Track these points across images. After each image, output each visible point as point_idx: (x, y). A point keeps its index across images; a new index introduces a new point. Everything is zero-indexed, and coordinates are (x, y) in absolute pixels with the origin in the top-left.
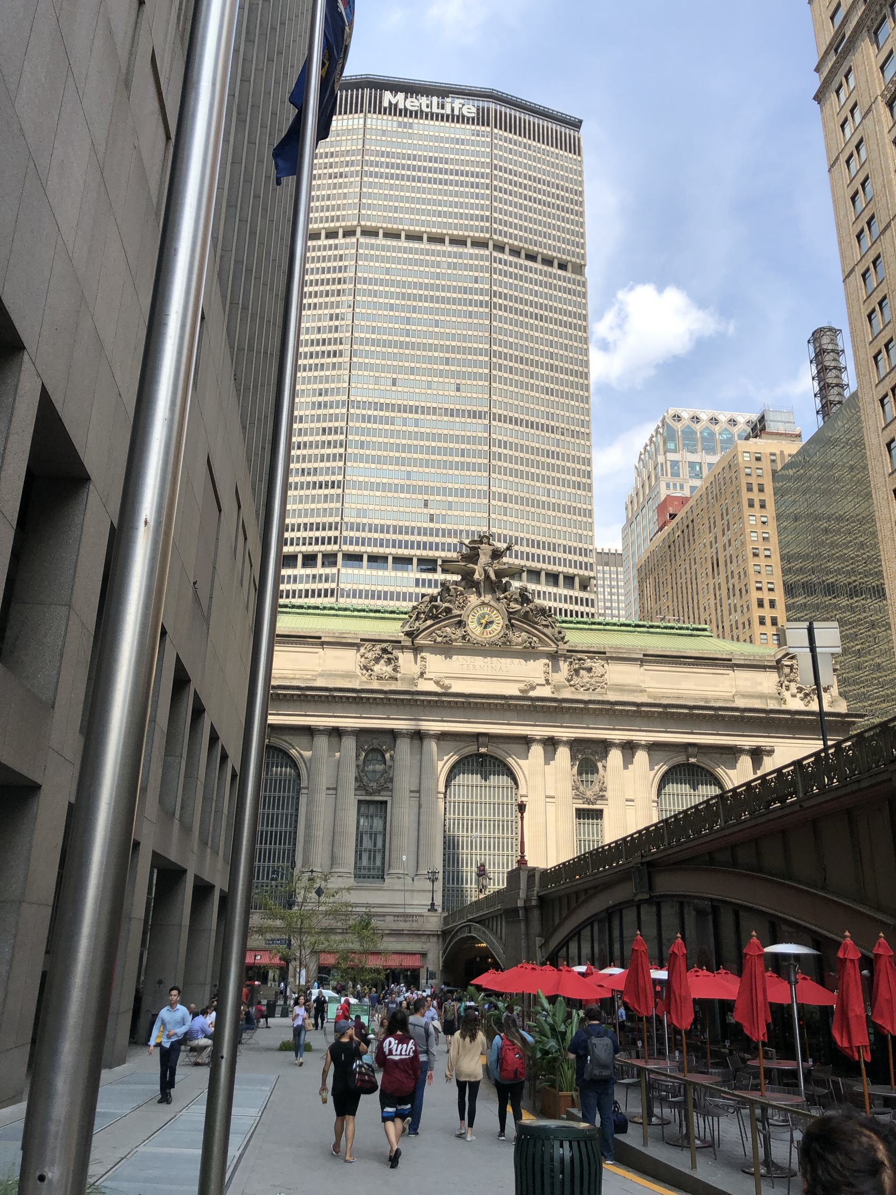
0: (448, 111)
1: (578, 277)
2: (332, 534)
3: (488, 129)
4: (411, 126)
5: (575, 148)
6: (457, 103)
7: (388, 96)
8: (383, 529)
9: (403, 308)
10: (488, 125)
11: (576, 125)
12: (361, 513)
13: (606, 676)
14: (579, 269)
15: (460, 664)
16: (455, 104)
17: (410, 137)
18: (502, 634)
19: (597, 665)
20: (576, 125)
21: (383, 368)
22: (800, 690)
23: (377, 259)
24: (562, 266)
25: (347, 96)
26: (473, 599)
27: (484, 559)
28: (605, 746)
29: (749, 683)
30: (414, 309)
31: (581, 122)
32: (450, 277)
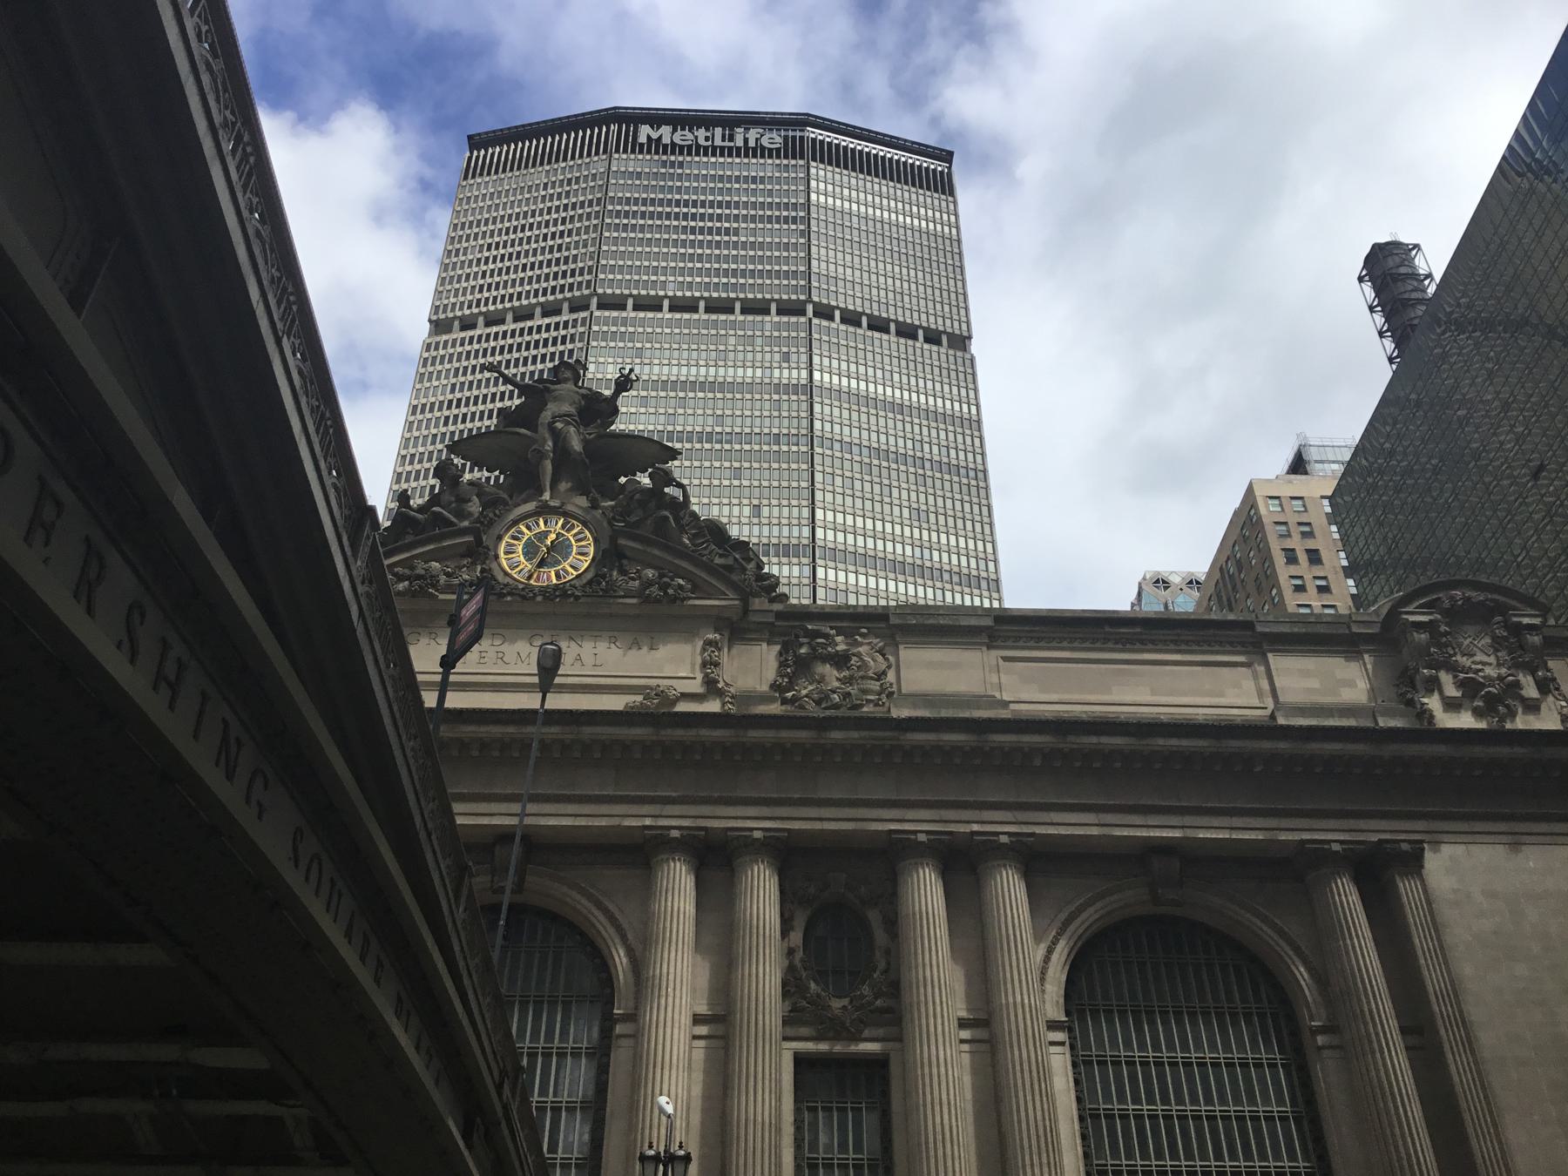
0: (739, 142)
1: (959, 354)
3: (801, 162)
5: (944, 186)
6: (753, 135)
7: (645, 131)
10: (802, 158)
11: (947, 157)
13: (891, 677)
14: (961, 342)
18: (590, 575)
20: (947, 157)
22: (1470, 687)
24: (933, 338)
25: (583, 138)
29: (1314, 683)
31: (951, 154)
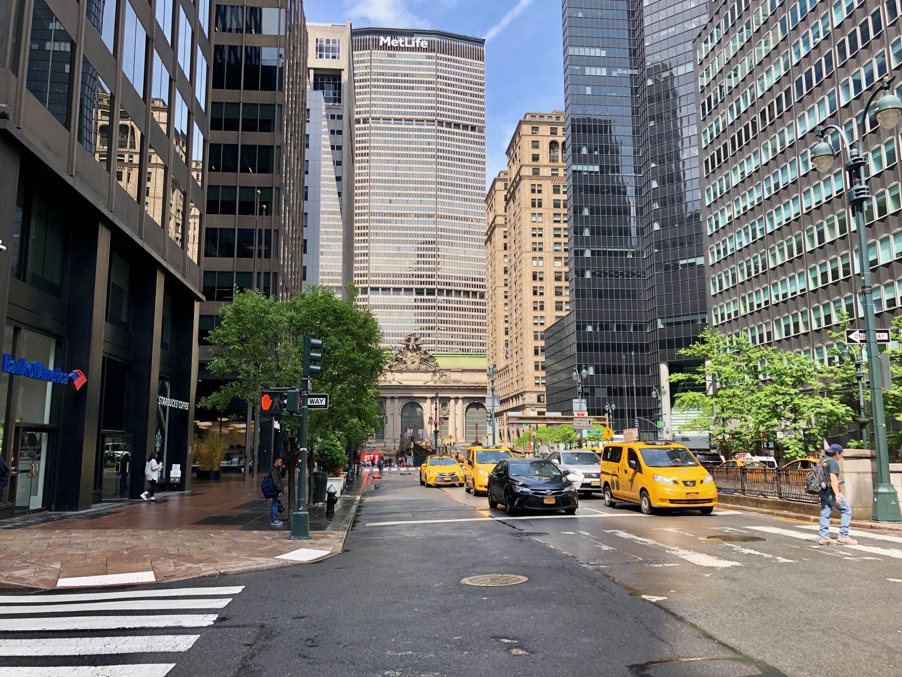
2: (365, 279)
4: (394, 56)
8: (388, 275)
9: (393, 162)
12: (378, 268)
15: (405, 375)
16: (418, 41)
17: (394, 62)
19: (448, 373)
21: (385, 195)
23: (380, 135)
26: (409, 354)
27: (412, 342)
28: (450, 399)
30: (399, 162)
32: (416, 143)
